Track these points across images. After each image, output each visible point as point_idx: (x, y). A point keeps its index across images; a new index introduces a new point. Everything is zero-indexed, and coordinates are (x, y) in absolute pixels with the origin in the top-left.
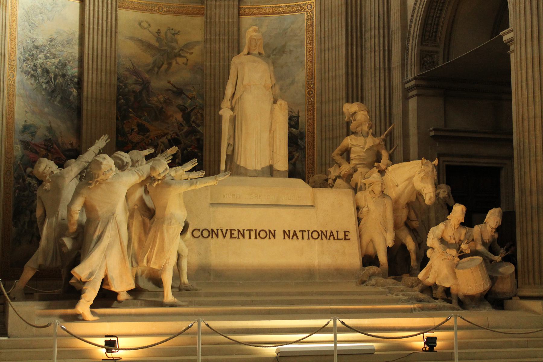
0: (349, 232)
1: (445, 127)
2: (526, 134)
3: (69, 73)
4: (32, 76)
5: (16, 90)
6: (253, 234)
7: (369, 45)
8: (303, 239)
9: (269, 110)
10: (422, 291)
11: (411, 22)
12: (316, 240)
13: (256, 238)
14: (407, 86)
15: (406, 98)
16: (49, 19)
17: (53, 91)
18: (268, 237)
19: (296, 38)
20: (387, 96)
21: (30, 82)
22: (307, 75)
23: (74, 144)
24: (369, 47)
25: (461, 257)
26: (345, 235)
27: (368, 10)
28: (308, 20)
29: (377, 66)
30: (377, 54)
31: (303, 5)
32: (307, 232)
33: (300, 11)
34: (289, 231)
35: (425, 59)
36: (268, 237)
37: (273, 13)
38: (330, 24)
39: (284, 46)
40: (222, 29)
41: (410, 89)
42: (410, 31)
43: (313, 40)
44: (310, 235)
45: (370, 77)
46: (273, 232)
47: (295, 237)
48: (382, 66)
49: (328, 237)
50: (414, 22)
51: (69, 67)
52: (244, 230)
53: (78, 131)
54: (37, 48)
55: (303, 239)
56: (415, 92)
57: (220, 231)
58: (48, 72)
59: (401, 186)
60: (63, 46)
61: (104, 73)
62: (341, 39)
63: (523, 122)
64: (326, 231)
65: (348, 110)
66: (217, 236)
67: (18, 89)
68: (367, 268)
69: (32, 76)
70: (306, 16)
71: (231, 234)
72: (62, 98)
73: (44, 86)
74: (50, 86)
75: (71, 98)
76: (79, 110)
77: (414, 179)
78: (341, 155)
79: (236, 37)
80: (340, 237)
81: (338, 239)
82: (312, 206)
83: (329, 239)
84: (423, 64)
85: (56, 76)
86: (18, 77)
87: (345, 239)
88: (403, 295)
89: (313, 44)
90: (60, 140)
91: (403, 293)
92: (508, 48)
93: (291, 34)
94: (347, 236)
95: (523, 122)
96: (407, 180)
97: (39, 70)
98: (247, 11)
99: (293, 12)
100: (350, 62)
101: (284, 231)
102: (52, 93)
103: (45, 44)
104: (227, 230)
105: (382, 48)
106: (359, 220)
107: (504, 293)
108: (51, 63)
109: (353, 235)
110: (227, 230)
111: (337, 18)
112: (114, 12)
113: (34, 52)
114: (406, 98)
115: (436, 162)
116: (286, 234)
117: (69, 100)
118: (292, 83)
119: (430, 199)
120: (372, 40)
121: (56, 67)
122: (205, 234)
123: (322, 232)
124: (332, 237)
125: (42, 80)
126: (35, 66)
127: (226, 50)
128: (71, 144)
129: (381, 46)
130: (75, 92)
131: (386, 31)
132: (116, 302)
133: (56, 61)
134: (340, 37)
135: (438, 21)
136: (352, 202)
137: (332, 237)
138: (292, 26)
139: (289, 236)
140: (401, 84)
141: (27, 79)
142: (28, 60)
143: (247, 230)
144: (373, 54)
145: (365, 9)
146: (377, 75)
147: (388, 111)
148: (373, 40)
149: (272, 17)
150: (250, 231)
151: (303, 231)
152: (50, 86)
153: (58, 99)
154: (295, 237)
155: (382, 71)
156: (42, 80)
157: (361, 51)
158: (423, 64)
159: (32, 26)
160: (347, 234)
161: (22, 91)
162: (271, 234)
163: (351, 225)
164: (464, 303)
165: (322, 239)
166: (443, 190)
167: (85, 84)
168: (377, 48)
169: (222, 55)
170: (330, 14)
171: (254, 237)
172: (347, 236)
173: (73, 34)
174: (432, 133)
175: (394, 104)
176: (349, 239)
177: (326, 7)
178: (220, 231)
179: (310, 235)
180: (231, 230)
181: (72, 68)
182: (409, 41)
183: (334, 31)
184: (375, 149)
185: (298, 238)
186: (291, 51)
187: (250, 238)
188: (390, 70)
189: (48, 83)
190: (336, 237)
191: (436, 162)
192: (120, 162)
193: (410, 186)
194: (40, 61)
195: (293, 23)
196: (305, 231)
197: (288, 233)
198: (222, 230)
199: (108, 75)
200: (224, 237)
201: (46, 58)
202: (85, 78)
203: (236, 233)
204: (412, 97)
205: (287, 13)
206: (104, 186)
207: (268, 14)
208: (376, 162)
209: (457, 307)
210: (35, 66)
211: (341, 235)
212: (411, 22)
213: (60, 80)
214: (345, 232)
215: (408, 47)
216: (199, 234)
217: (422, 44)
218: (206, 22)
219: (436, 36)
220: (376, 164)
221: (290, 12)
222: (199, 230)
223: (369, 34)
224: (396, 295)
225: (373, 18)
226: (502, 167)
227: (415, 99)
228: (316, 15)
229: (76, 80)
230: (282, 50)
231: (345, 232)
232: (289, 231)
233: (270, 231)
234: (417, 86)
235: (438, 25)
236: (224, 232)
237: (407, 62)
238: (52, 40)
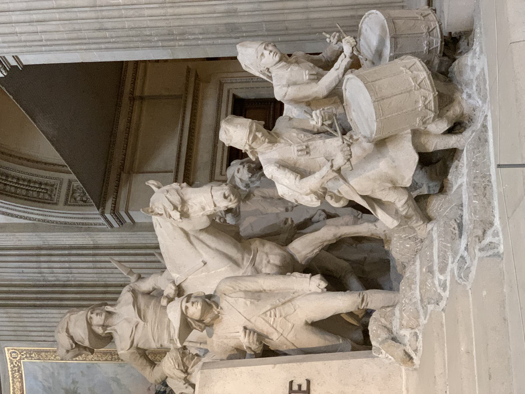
0: (291, 383)
1: (172, 172)
7: (63, 275)
11: (30, 219)
14: (115, 225)
19: (56, 374)
20: (132, 252)
22: (106, 360)
24: (65, 275)
25: (345, 130)
28: (32, 357)
29: (91, 265)
31: (12, 363)
35: (78, 199)
38: (35, 329)
41: (121, 222)
42: (39, 220)
45: (106, 275)
48: (91, 259)
50: (26, 215)
59: (207, 255)
63: (106, 29)
65: (68, 351)
68: (373, 343)
70: (26, 360)
77: (187, 228)
78: (153, 364)
84: (85, 201)
88: (442, 271)
91: (436, 268)
93: (51, 380)
94: (300, 386)
95: (106, 29)
96: (191, 242)
99: (21, 377)
105: (67, 259)
106: (267, 352)
107: (430, 32)
109: (299, 370)
111: (26, 320)
115: (152, 183)
118: (117, 381)
119: (225, 197)
120: (56, 272)
134: (49, 315)
135: (24, 180)
136: (225, 370)
138: (40, 379)
140: (114, 233)
144: (74, 271)
145: (15, 280)
148: (55, 270)
155: (98, 258)
157: (71, 286)
158: (85, 201)
160: (295, 388)
166: (236, 173)
168: (67, 265)
170: (21, 329)
172: (300, 386)
175: (144, 242)
176: (308, 382)
177: (13, 333)
182: (53, 222)
183: (43, 324)
184: (142, 301)
186: (74, 382)
191: (152, 183)
193: (204, 236)
195: (36, 378)
205: (22, 385)
209: (467, 133)
212: (26, 218)
215: (61, 223)
217: (56, 204)
219: (46, 184)
221: (22, 382)
223: (47, 275)
224: (444, 290)
225: (25, 270)
226: (234, 96)
234: (114, 211)
235: (29, 181)
237: (83, 224)
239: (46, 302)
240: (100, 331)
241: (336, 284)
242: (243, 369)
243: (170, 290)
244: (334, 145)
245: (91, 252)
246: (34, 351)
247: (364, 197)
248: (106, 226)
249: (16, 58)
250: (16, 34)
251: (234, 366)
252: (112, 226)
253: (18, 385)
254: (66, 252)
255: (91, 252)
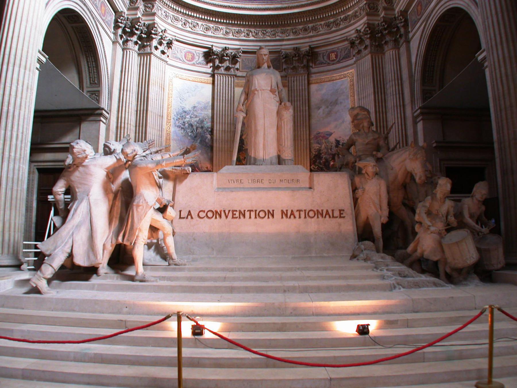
0: (343, 210)
2: (505, 122)
3: (205, 126)
4: (182, 128)
5: (171, 136)
6: (253, 214)
8: (300, 217)
9: (276, 112)
10: (411, 266)
11: (415, 74)
12: (313, 219)
13: (256, 217)
14: (415, 114)
15: (415, 123)
16: (193, 96)
17: (195, 137)
18: (267, 216)
21: (180, 132)
23: (209, 168)
25: (448, 231)
26: (340, 214)
27: (387, 70)
29: (395, 104)
30: (395, 96)
32: (304, 212)
33: (345, 77)
34: (287, 211)
36: (267, 216)
37: (330, 81)
39: (337, 100)
40: (298, 94)
43: (354, 94)
44: (307, 214)
46: (272, 212)
47: (292, 216)
49: (324, 215)
51: (205, 123)
52: (245, 211)
53: (211, 160)
54: (185, 112)
55: (300, 217)
56: (421, 118)
57: (223, 213)
58: (192, 126)
60: (201, 110)
61: (226, 125)
62: (370, 90)
63: (501, 113)
64: (322, 210)
66: (220, 216)
67: (172, 136)
69: (182, 128)
71: (233, 214)
72: (201, 141)
73: (190, 134)
74: (193, 134)
75: (207, 140)
76: (212, 148)
79: (307, 97)
80: (335, 215)
81: (333, 217)
82: (310, 188)
83: (325, 217)
85: (197, 128)
86: (172, 129)
87: (340, 217)
88: (387, 270)
89: (354, 96)
90: (200, 166)
92: (483, 65)
94: (342, 214)
95: (501, 113)
97: (187, 125)
98: (313, 82)
100: (377, 104)
101: (282, 212)
102: (195, 138)
103: (191, 109)
104: (229, 211)
105: (397, 93)
106: (355, 200)
108: (194, 121)
110: (229, 211)
112: (232, 89)
113: (184, 114)
114: (415, 123)
116: (284, 214)
117: (205, 142)
118: (343, 122)
119: (420, 178)
120: (391, 89)
121: (197, 123)
122: (210, 214)
123: (318, 210)
124: (327, 216)
125: (188, 131)
126: (184, 123)
127: (301, 106)
128: (207, 168)
129: (397, 91)
130: (209, 137)
131: (400, 82)
132: (95, 275)
133: (198, 119)
136: (347, 183)
137: (327, 216)
139: (286, 215)
141: (179, 130)
142: (179, 119)
143: (248, 211)
146: (396, 110)
147: (404, 133)
149: (328, 83)
150: (250, 211)
151: (299, 211)
152: (193, 134)
153: (199, 141)
154: (292, 216)
155: (399, 107)
156: (188, 131)
157: (385, 96)
159: (182, 99)
160: (342, 212)
161: (175, 137)
162: (271, 214)
163: (346, 203)
164: (453, 276)
165: (318, 217)
167: (215, 132)
168: (394, 93)
169: (299, 109)
171: (254, 217)
173: (208, 103)
174: (434, 145)
176: (344, 217)
178: (223, 213)
179: (307, 214)
180: (233, 211)
181: (207, 123)
182: (414, 85)
185: (295, 217)
186: (341, 103)
187: (250, 217)
188: (404, 106)
189: (192, 132)
190: (331, 216)
192: (107, 149)
194: (187, 120)
195: (342, 85)
196: (302, 211)
197: (285, 212)
198: (224, 211)
199: (229, 126)
200: (227, 217)
201: (191, 117)
202: (215, 128)
203: (237, 214)
204: (419, 121)
206: (81, 169)
207: (326, 82)
208: (374, 151)
210: (184, 123)
211: (336, 214)
213: (200, 130)
214: (340, 211)
215: (414, 88)
216: (204, 214)
218: (289, 90)
220: (374, 153)
221: (339, 79)
222: (204, 211)
225: (390, 75)
227: (421, 122)
228: (355, 78)
229: (210, 130)
230: (336, 103)
231: (340, 211)
232: (287, 211)
233: (269, 211)
236: (227, 212)
238: (195, 107)
239: (376, 86)
240: (361, 126)
241: (384, 227)
242: (348, 191)
243: (380, 155)
244: (440, 226)
245: (401, 104)
246: (353, 83)
247: (419, 238)
248: (414, 111)
249: (487, 67)
250: (495, 70)
251: (349, 187)
252: (414, 113)
253: (338, 78)
254: (400, 92)
255: (401, 104)
